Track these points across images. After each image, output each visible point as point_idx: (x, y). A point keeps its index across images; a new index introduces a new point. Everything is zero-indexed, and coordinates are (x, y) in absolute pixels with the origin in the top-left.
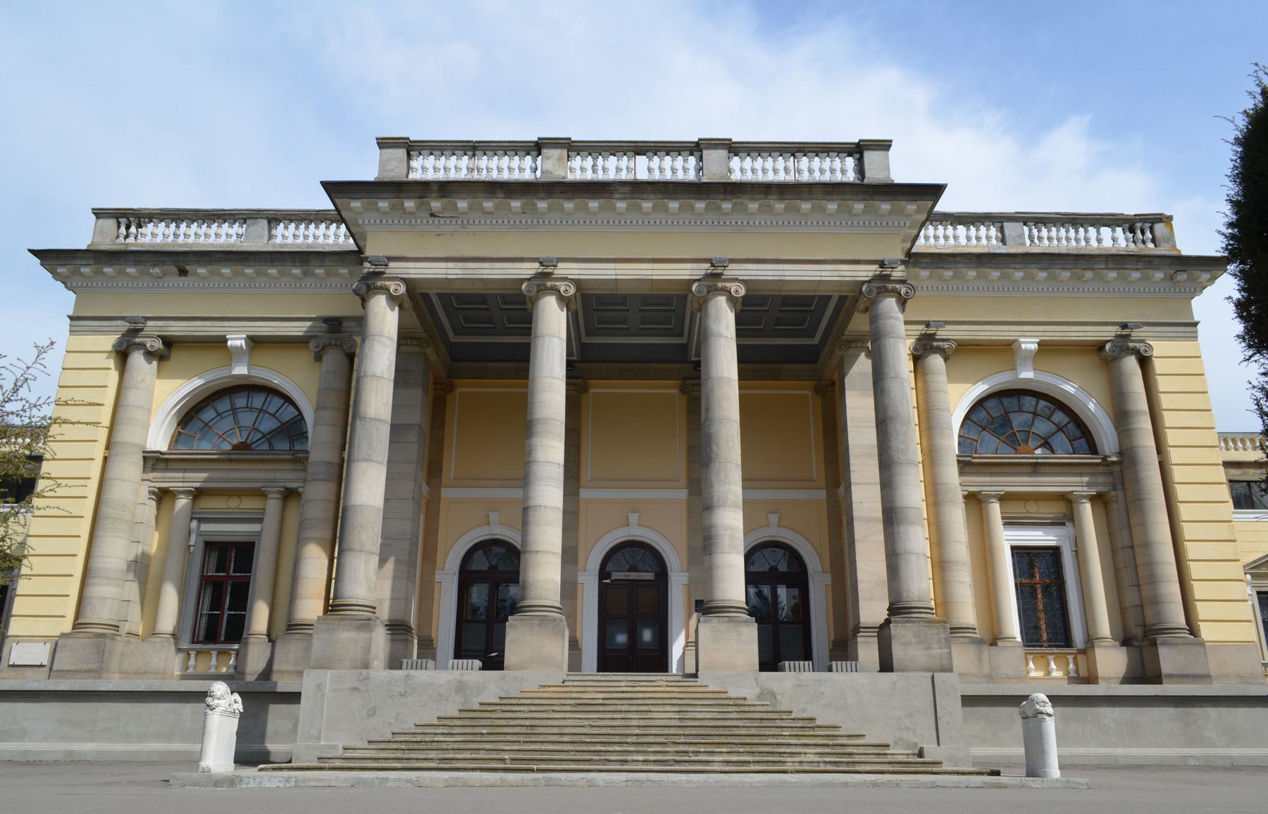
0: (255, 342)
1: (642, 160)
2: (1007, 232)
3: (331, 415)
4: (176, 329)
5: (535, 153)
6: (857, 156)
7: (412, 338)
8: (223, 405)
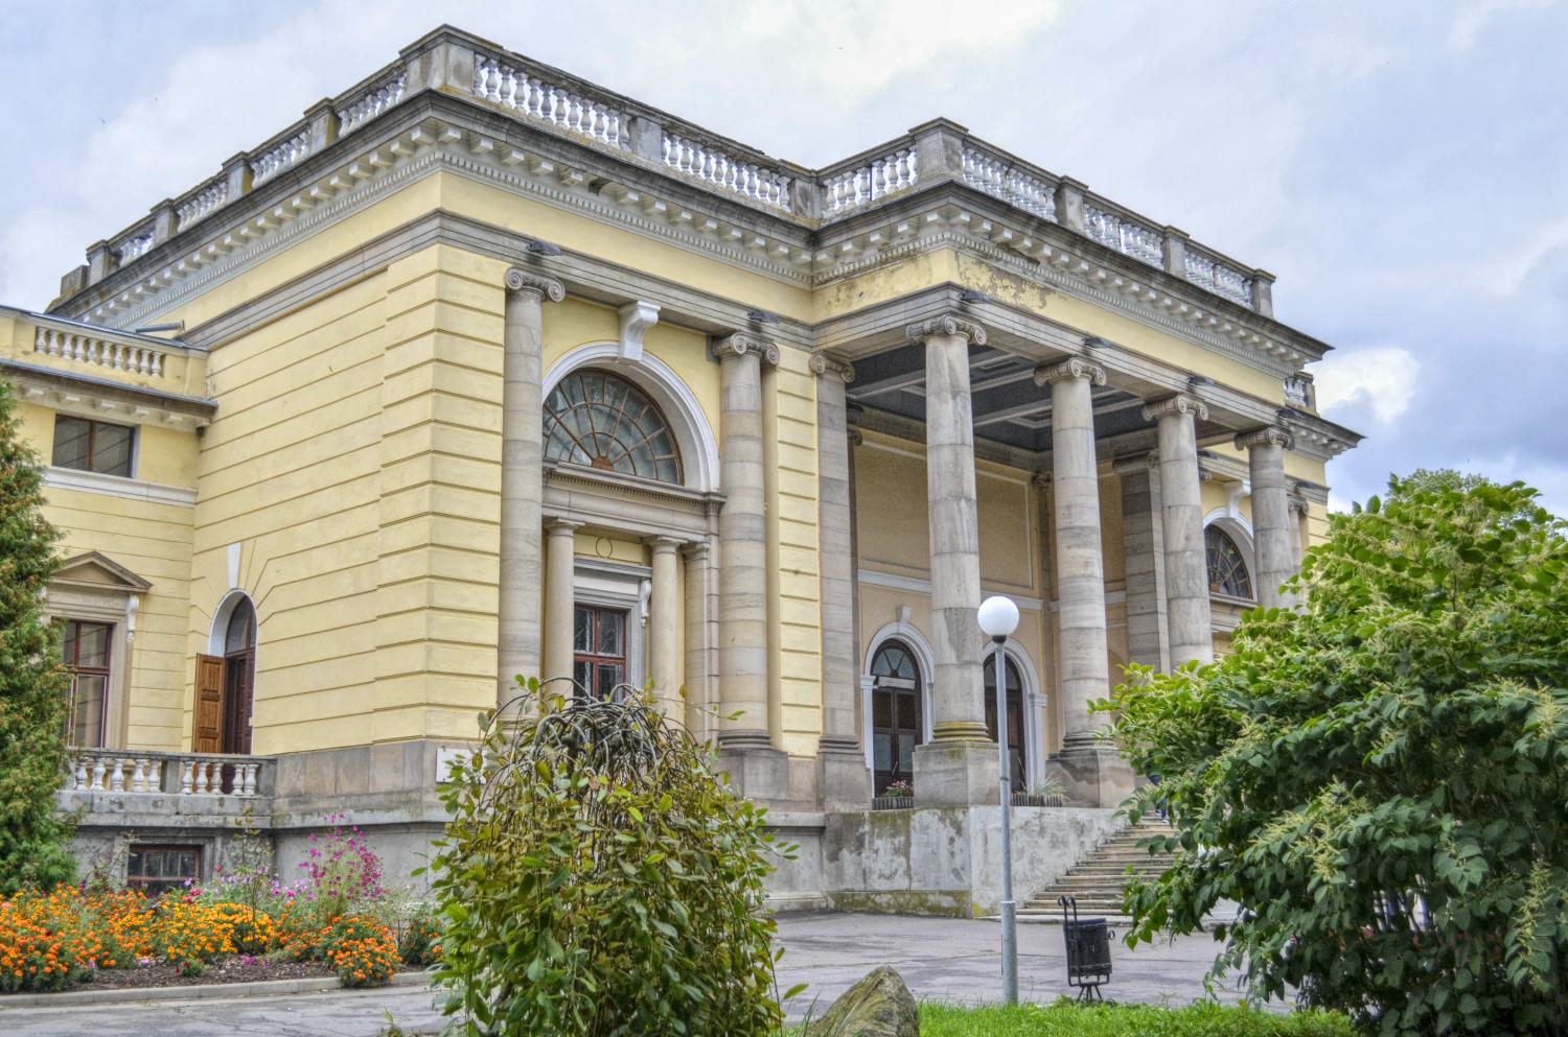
0: (670, 321)
4: (580, 273)
7: (837, 362)
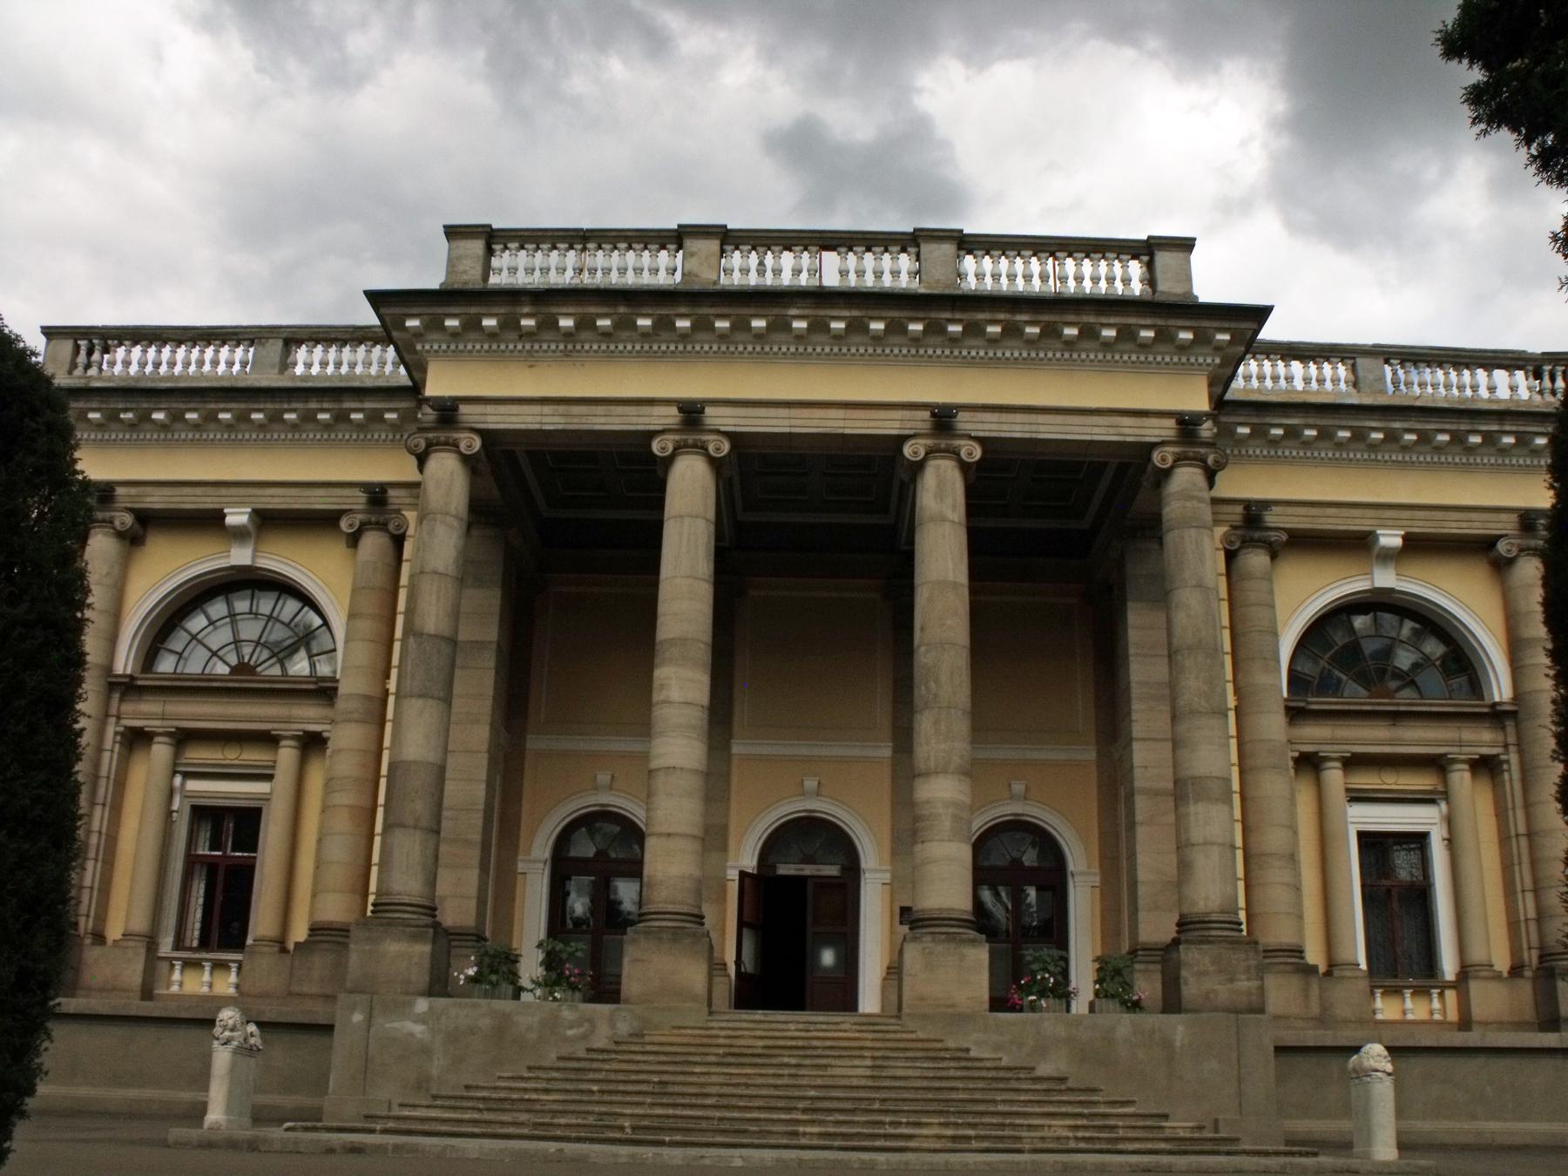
1: (831, 259)
2: (1361, 373)
3: (366, 627)
4: (156, 500)
5: (672, 247)
6: (1145, 258)
8: (218, 608)
